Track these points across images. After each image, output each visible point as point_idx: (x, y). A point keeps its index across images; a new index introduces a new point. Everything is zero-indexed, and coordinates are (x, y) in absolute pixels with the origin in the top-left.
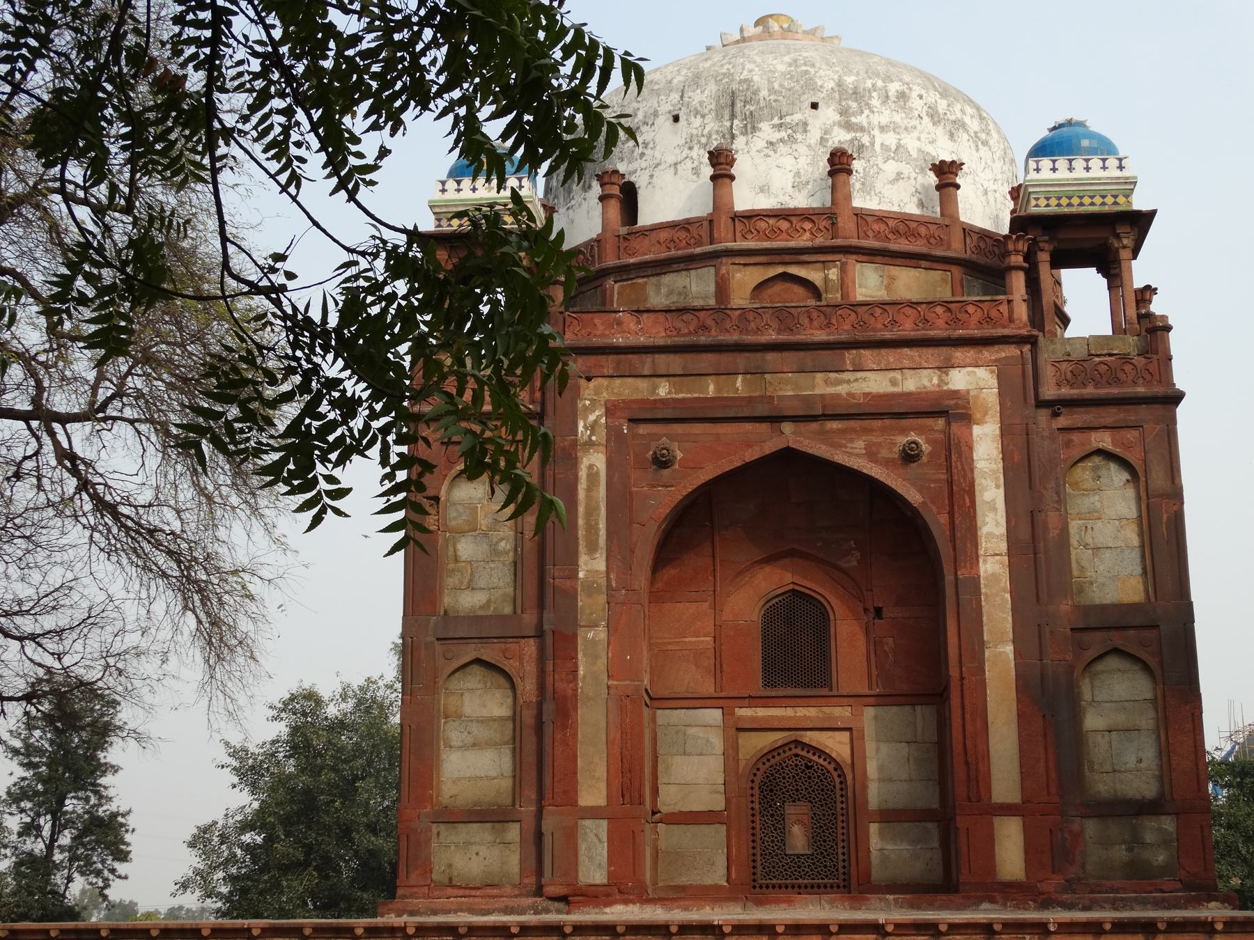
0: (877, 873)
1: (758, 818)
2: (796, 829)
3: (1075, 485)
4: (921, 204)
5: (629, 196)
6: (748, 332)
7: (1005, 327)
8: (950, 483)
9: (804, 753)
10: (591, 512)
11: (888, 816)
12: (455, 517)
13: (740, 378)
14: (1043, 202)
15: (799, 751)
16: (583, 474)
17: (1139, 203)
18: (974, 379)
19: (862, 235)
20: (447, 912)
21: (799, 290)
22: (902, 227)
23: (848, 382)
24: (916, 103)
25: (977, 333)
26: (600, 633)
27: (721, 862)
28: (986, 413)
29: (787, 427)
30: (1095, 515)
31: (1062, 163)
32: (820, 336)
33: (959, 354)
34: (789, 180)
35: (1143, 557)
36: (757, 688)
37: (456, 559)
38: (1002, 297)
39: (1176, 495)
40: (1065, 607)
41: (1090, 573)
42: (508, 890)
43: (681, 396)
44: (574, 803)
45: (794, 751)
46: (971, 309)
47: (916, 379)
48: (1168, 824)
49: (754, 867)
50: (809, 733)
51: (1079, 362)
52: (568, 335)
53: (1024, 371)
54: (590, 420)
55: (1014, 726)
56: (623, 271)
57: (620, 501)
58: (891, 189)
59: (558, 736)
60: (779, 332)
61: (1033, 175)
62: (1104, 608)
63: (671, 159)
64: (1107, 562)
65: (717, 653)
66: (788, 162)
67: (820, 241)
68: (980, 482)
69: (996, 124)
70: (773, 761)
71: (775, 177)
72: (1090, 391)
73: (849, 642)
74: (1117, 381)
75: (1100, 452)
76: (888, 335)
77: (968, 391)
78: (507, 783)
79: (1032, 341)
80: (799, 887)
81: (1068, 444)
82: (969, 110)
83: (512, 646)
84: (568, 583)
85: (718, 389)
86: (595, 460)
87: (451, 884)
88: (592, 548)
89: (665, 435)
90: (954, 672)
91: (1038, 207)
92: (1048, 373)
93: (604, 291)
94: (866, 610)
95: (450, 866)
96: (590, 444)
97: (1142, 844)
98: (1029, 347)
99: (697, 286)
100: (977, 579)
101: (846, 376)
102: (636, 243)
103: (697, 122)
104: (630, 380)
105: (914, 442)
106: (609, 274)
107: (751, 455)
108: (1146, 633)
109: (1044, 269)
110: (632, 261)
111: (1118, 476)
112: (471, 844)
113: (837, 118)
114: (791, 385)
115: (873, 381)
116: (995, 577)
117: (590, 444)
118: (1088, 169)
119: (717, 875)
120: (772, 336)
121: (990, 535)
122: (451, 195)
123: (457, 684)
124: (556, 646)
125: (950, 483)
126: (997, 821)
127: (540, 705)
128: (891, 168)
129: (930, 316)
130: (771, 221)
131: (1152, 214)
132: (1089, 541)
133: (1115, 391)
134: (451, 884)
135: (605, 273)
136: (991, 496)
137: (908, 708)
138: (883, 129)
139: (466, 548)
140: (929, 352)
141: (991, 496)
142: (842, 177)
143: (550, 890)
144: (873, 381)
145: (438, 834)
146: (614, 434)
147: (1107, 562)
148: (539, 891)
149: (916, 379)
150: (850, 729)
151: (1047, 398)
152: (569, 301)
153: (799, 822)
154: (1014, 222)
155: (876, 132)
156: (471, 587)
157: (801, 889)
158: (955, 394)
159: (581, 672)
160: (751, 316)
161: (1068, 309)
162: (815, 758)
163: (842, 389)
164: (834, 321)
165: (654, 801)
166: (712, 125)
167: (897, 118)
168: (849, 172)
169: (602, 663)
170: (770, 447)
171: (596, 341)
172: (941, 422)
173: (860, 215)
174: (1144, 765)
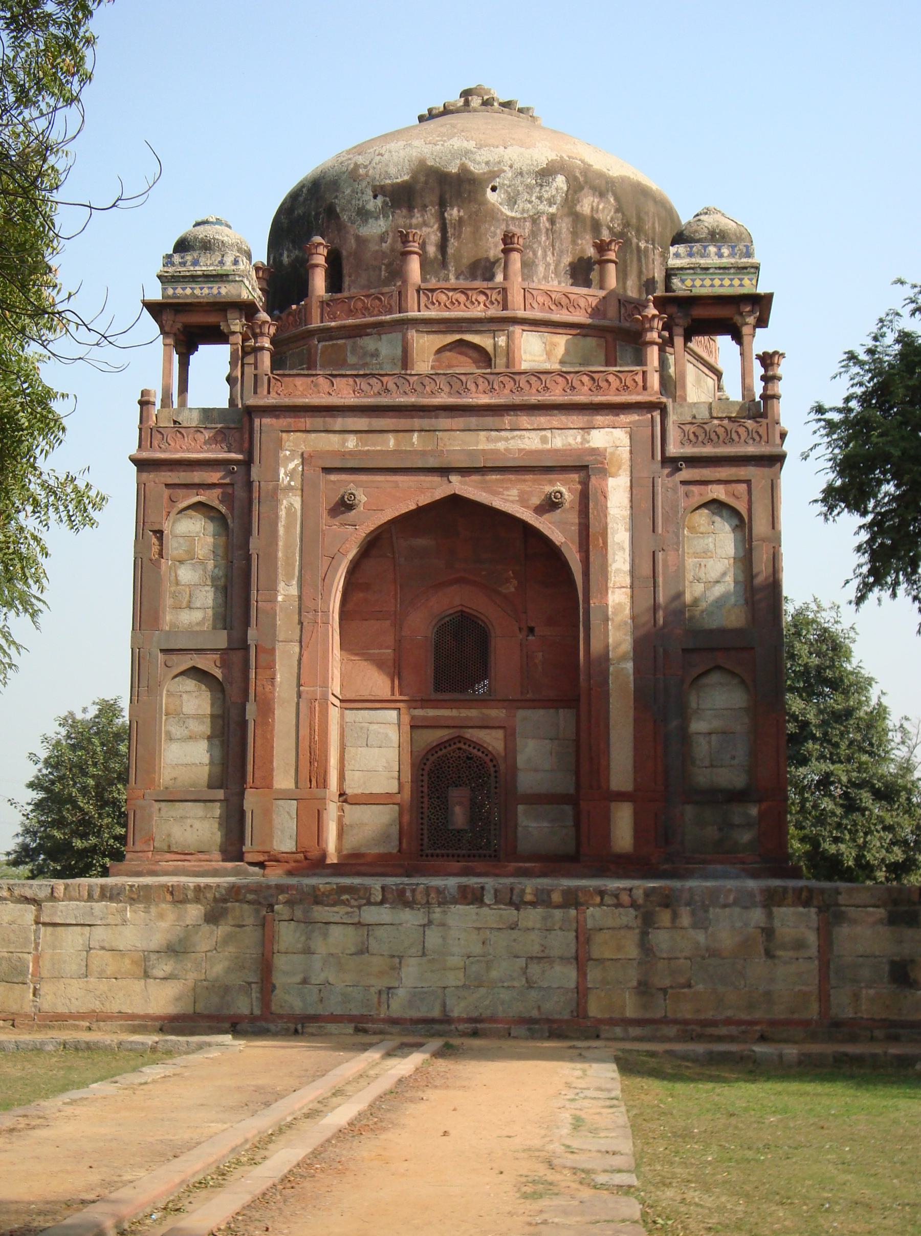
0: (523, 846)
1: (426, 800)
2: (458, 810)
3: (692, 529)
6: (423, 395)
7: (639, 394)
9: (466, 747)
13: (416, 435)
15: (461, 745)
16: (283, 513)
17: (761, 290)
18: (610, 438)
19: (528, 306)
22: (564, 301)
23: (507, 439)
28: (619, 468)
29: (454, 478)
30: (706, 553)
32: (484, 400)
33: (599, 419)
37: (177, 583)
38: (638, 368)
43: (366, 448)
44: (269, 786)
45: (458, 745)
46: (611, 378)
49: (422, 840)
50: (470, 730)
51: (701, 425)
52: (273, 394)
55: (630, 729)
62: (711, 631)
70: (440, 753)
75: (714, 501)
77: (605, 449)
80: (459, 856)
85: (398, 442)
88: (289, 577)
89: (353, 482)
93: (309, 351)
94: (520, 629)
95: (169, 835)
96: (289, 488)
98: (659, 411)
101: (503, 434)
104: (323, 434)
105: (559, 492)
106: (314, 335)
107: (424, 500)
110: (333, 324)
112: (187, 818)
118: (721, 256)
121: (618, 571)
126: (613, 805)
129: (576, 383)
130: (450, 294)
131: (769, 298)
132: (702, 575)
137: (552, 711)
143: (249, 857)
145: (160, 809)
150: (504, 727)
151: (672, 455)
158: (594, 451)
159: (278, 678)
161: (720, 366)
162: (475, 751)
163: (501, 446)
164: (496, 387)
174: (736, 762)
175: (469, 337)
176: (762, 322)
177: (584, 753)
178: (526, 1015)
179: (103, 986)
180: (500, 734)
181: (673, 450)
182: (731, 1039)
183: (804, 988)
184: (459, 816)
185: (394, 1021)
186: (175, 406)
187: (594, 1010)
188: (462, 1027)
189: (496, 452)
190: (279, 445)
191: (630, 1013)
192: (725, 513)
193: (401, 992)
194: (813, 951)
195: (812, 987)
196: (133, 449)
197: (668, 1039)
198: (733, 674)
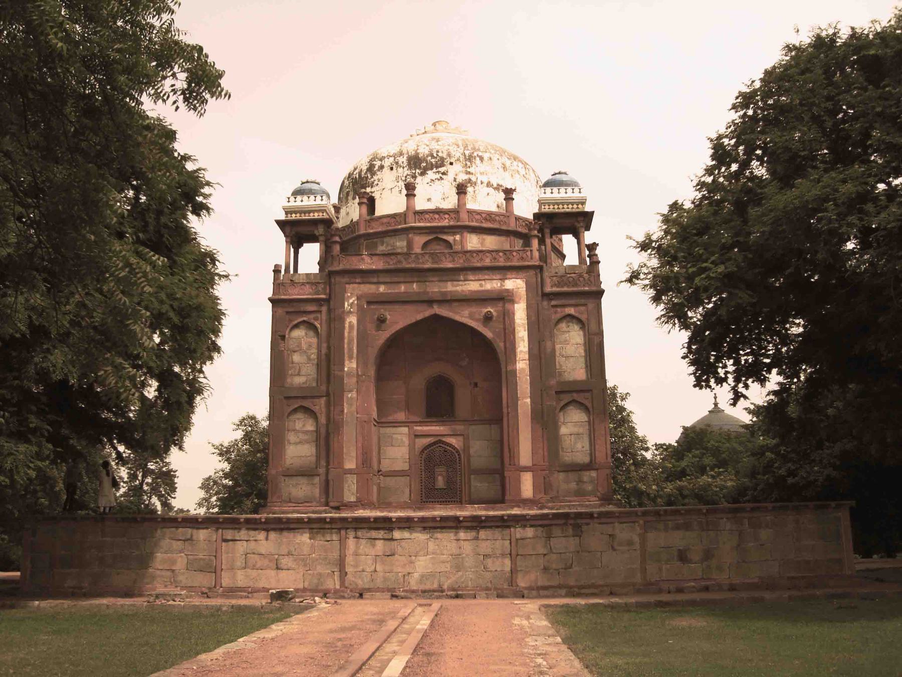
2: (440, 478)
3: (559, 330)
4: (498, 207)
5: (371, 203)
8: (505, 329)
11: (479, 472)
12: (292, 344)
14: (547, 207)
16: (347, 325)
17: (587, 208)
18: (515, 284)
20: (288, 513)
21: (441, 243)
25: (517, 264)
26: (354, 394)
27: (407, 491)
30: (566, 342)
31: (555, 190)
32: (450, 265)
34: (441, 196)
35: (586, 361)
37: (293, 363)
39: (600, 333)
40: (553, 382)
44: (343, 468)
46: (515, 254)
47: (491, 285)
48: (594, 474)
53: (537, 281)
54: (350, 302)
56: (368, 236)
57: (363, 337)
58: (483, 200)
59: (335, 439)
60: (433, 263)
61: (543, 196)
62: (570, 382)
67: (452, 223)
68: (518, 329)
71: (435, 194)
72: (565, 289)
73: (463, 397)
74: (576, 285)
75: (569, 315)
76: (479, 265)
78: (314, 459)
79: (540, 268)
82: (520, 164)
83: (317, 400)
84: (340, 373)
86: (353, 320)
88: (351, 358)
90: (505, 410)
91: (546, 209)
92: (548, 281)
96: (350, 312)
99: (400, 244)
100: (514, 372)
101: (461, 283)
102: (373, 224)
103: (400, 170)
107: (420, 317)
108: (588, 395)
109: (547, 235)
111: (576, 327)
113: (461, 169)
114: (435, 288)
115: (472, 286)
116: (523, 369)
117: (350, 312)
119: (405, 497)
120: (427, 266)
121: (521, 351)
122: (292, 204)
123: (293, 417)
125: (505, 329)
127: (327, 425)
129: (497, 257)
131: (591, 214)
133: (575, 289)
135: (360, 236)
136: (522, 335)
137: (488, 426)
139: (296, 358)
141: (522, 335)
142: (462, 195)
144: (472, 286)
146: (360, 307)
148: (327, 505)
149: (491, 285)
153: (441, 475)
154: (535, 215)
155: (478, 175)
156: (299, 375)
157: (441, 503)
158: (507, 290)
160: (420, 257)
161: (565, 252)
163: (459, 288)
165: (379, 466)
166: (407, 172)
168: (465, 193)
169: (354, 408)
170: (428, 313)
171: (353, 267)
172: (500, 304)
173: (470, 212)
176: (588, 228)
178: (484, 586)
179: (254, 573)
180: (461, 438)
181: (548, 289)
182: (594, 595)
183: (634, 566)
184: (440, 482)
185: (413, 592)
186: (292, 272)
187: (522, 582)
188: (449, 593)
189: (457, 291)
191: (540, 584)
193: (416, 575)
194: (638, 546)
196: (270, 294)
198: (581, 404)
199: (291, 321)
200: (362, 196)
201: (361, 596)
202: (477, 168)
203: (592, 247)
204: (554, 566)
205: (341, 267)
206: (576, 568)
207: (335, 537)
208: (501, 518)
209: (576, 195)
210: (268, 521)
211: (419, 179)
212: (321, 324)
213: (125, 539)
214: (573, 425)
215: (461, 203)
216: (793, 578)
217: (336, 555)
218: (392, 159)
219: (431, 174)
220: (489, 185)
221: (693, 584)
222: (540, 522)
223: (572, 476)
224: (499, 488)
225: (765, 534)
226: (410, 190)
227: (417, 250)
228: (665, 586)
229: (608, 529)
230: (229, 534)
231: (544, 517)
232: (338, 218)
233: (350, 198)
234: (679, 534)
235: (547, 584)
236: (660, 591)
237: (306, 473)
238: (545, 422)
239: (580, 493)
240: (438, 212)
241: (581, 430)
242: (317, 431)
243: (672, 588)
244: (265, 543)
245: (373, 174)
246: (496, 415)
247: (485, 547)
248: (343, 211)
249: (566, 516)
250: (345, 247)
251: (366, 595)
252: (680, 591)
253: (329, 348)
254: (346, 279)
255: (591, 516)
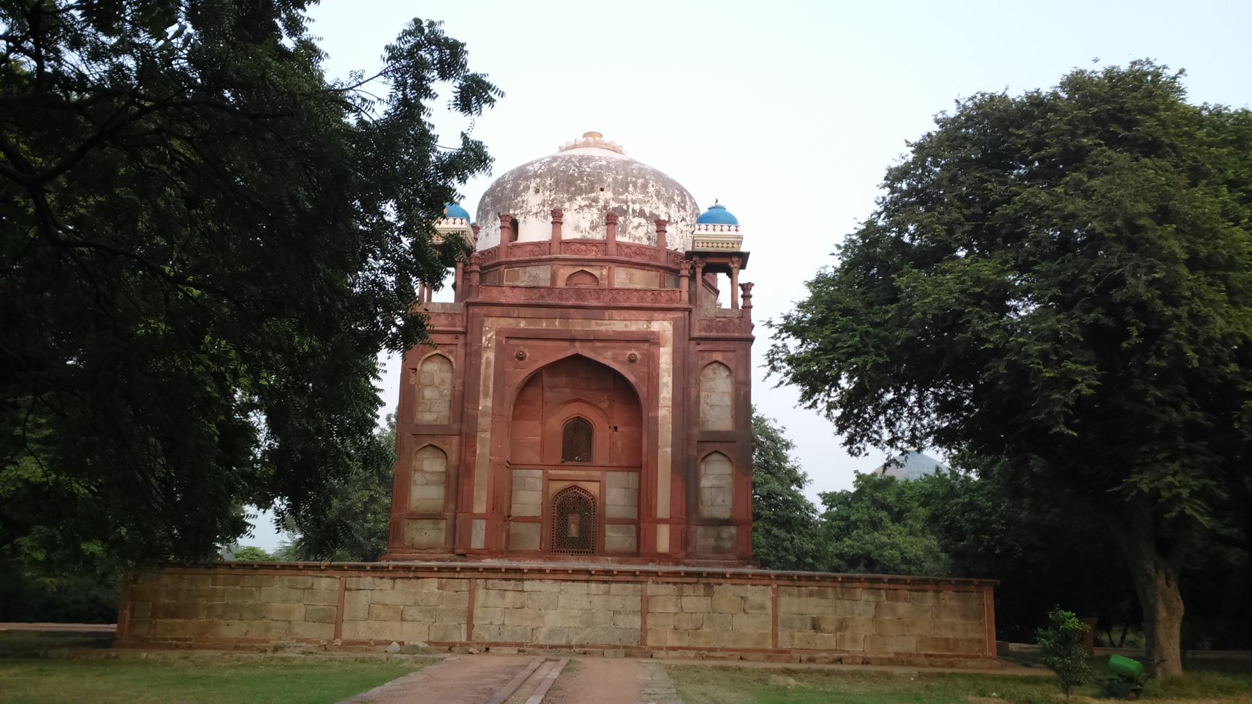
3: (705, 376)
5: (513, 226)
8: (649, 373)
10: (487, 378)
12: (425, 380)
16: (483, 361)
17: (743, 249)
18: (662, 326)
21: (588, 279)
24: (651, 190)
26: (488, 435)
29: (577, 344)
30: (712, 390)
31: (710, 227)
32: (595, 303)
33: (656, 315)
36: (558, 459)
41: (708, 417)
42: (439, 550)
44: (471, 512)
48: (733, 530)
54: (489, 337)
56: (510, 264)
57: (500, 376)
58: (637, 233)
63: (534, 210)
64: (716, 411)
65: (542, 445)
66: (588, 216)
67: (600, 256)
69: (691, 198)
71: (580, 223)
72: (713, 334)
74: (727, 331)
76: (625, 304)
78: (441, 502)
79: (690, 311)
81: (703, 357)
86: (490, 355)
87: (413, 547)
88: (486, 396)
90: (644, 459)
91: (700, 248)
92: (697, 324)
96: (487, 347)
97: (722, 539)
99: (542, 275)
102: (515, 251)
107: (561, 356)
111: (723, 373)
117: (487, 347)
119: (535, 545)
123: (419, 456)
124: (468, 440)
125: (649, 373)
127: (458, 467)
128: (637, 221)
134: (413, 547)
135: (500, 264)
138: (634, 202)
139: (428, 393)
140: (643, 313)
146: (498, 343)
147: (716, 411)
149: (636, 325)
152: (482, 281)
156: (430, 411)
161: (719, 287)
163: (603, 328)
167: (641, 196)
169: (487, 450)
170: (569, 353)
172: (646, 345)
173: (619, 245)
175: (586, 269)
176: (743, 267)
177: (643, 496)
181: (696, 334)
182: (722, 658)
184: (573, 531)
185: (541, 647)
187: (650, 642)
188: (577, 650)
190: (482, 324)
191: (669, 644)
192: (722, 368)
193: (544, 630)
194: (770, 611)
195: (769, 630)
197: (689, 658)
199: (423, 353)
200: (503, 218)
201: (487, 649)
202: (632, 195)
203: (747, 287)
204: (684, 626)
205: (480, 298)
206: (705, 629)
207: (464, 585)
208: (633, 573)
209: (733, 233)
210: (396, 568)
211: (567, 205)
212: (456, 358)
213: (238, 587)
214: (716, 477)
215: (610, 235)
216: (931, 656)
217: (464, 606)
218: (538, 180)
219: (580, 201)
220: (642, 214)
221: (825, 654)
222: (671, 580)
223: (711, 531)
224: (634, 541)
225: (902, 608)
226: (557, 217)
227: (561, 284)
228: (796, 655)
229: (740, 590)
230: (353, 582)
231: (677, 574)
232: (476, 239)
233: (491, 217)
234: (814, 600)
235: (677, 644)
236: (790, 660)
237: (431, 517)
238: (687, 473)
239: (718, 550)
240: (584, 242)
241: (723, 483)
242: (447, 472)
243: (804, 657)
244: (391, 592)
245: (518, 194)
246: (638, 463)
247: (616, 603)
248: (482, 234)
249: (699, 575)
250: (484, 271)
251: (493, 650)
252: (811, 660)
253: (464, 384)
254: (484, 310)
255: (723, 576)
